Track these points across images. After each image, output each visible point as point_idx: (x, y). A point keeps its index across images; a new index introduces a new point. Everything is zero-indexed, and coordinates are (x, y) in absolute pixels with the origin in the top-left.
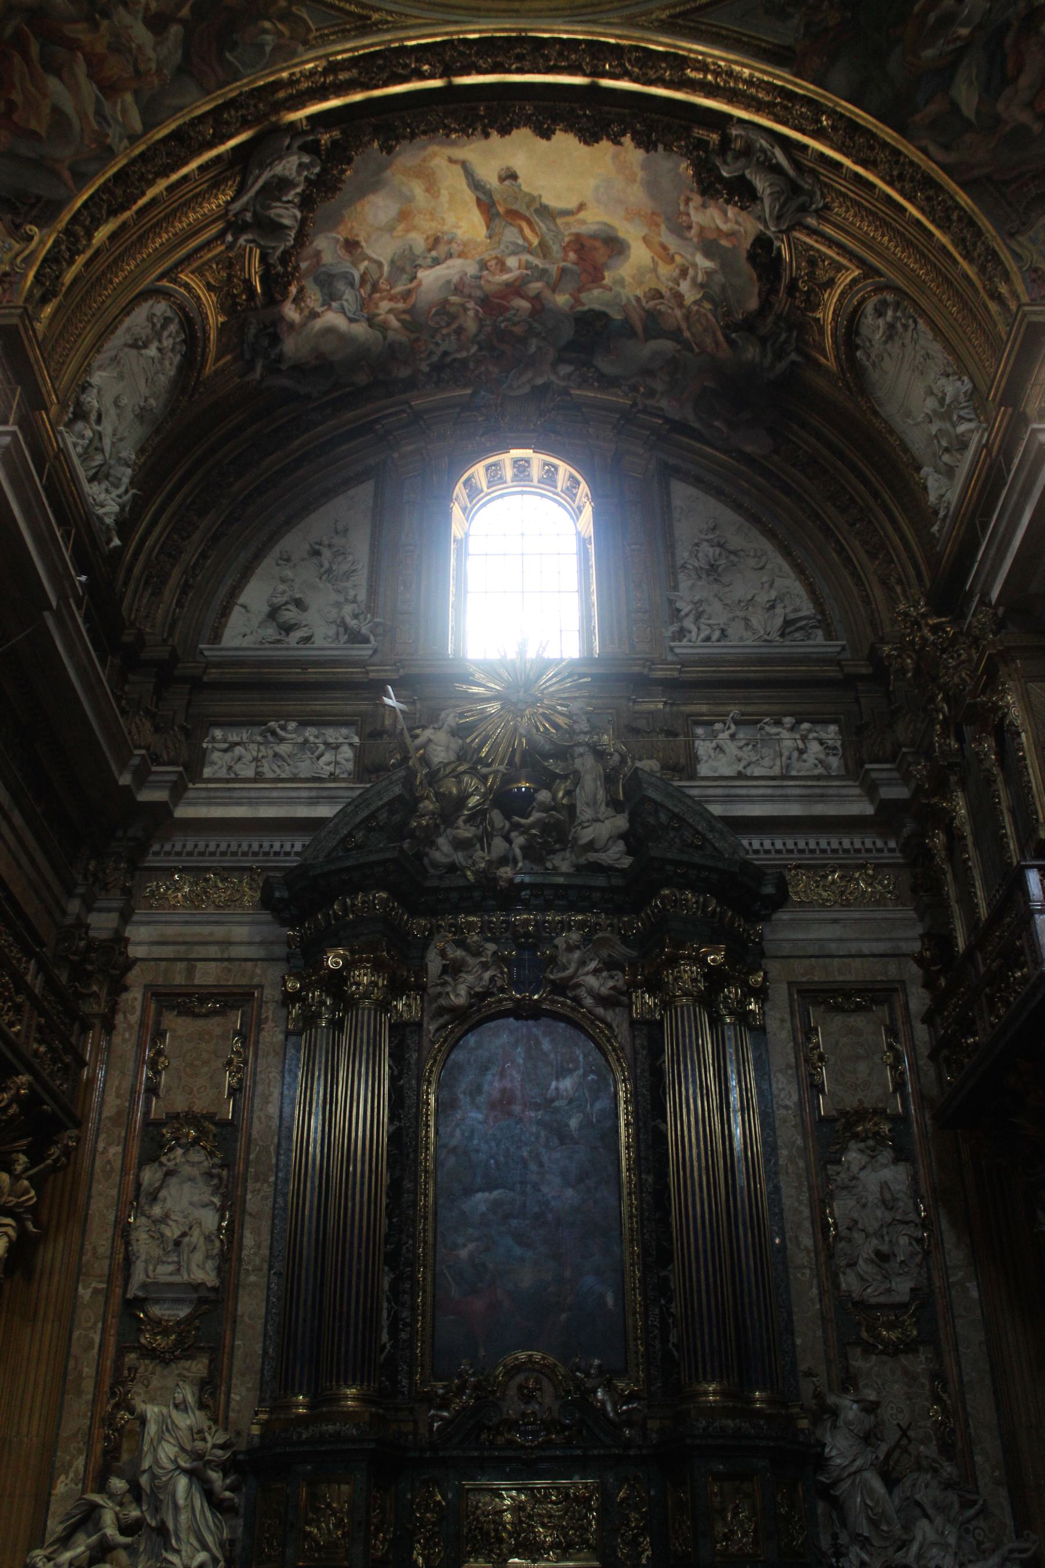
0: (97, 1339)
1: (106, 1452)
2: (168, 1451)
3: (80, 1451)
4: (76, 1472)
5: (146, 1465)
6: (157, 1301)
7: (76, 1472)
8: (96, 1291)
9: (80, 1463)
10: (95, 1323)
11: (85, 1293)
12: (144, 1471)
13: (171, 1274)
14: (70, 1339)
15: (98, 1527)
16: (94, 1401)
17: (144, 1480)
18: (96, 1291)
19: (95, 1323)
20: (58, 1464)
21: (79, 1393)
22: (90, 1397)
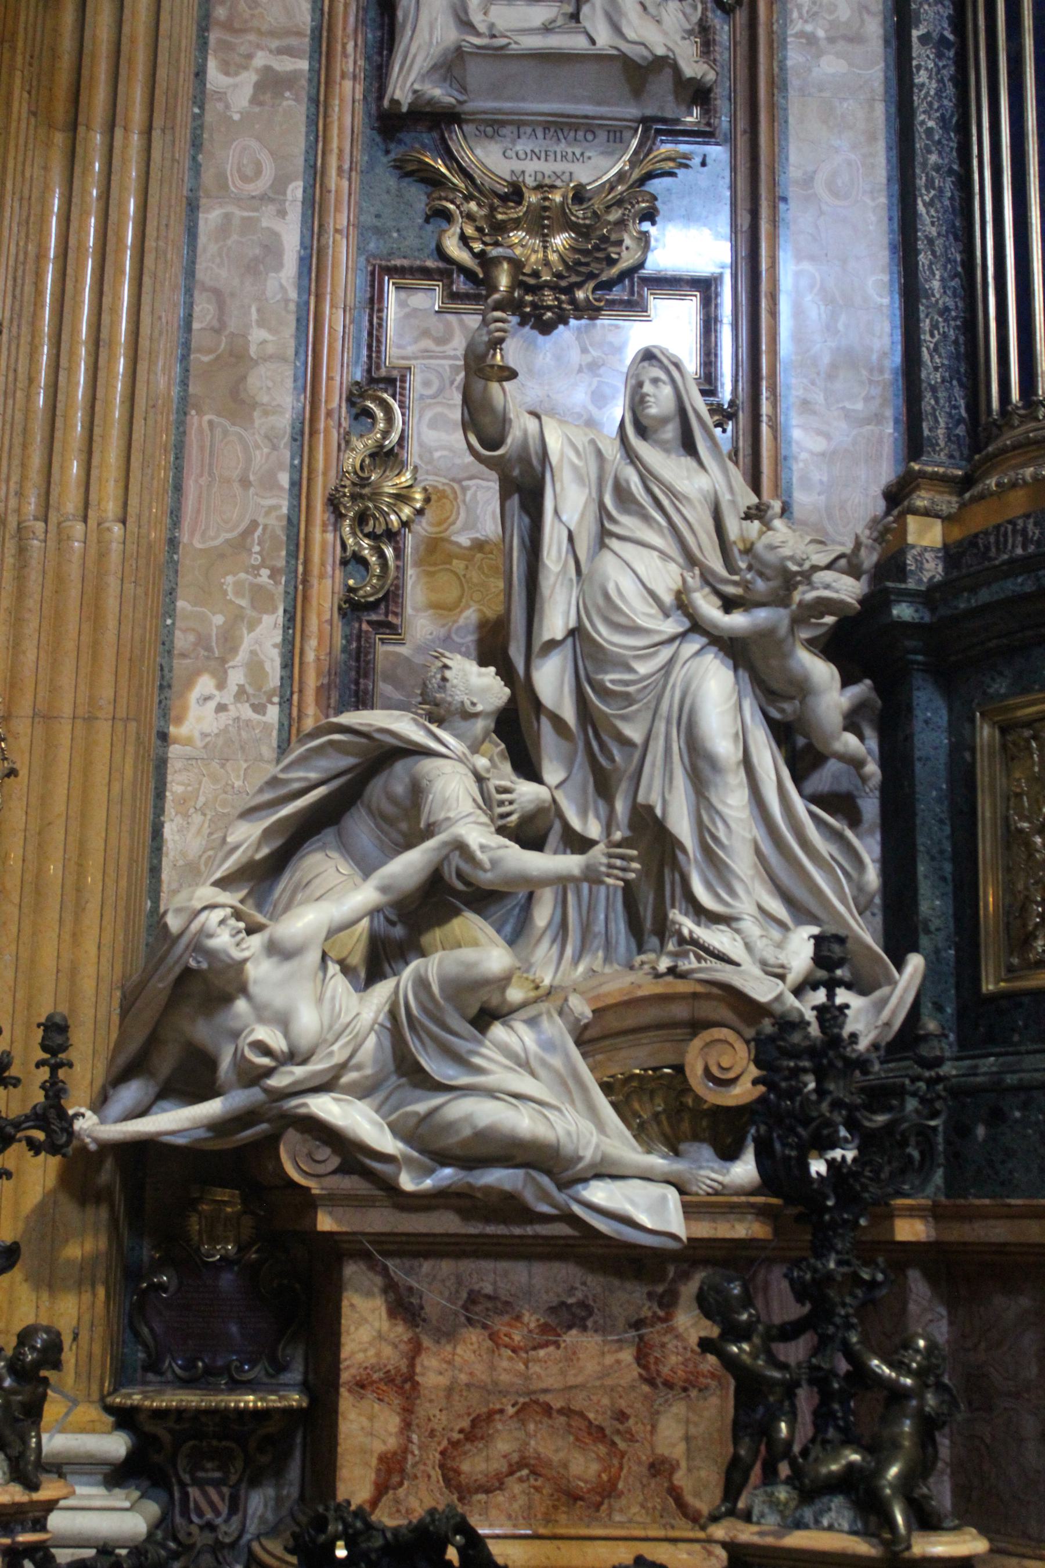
0: (291, 235)
1: (352, 607)
2: (642, 575)
3: (260, 598)
4: (255, 668)
5: (556, 622)
6: (494, 126)
7: (255, 668)
8: (271, 84)
9: (265, 637)
10: (280, 185)
11: (232, 88)
12: (552, 645)
13: (547, 29)
14: (192, 233)
15: (409, 824)
16: (305, 433)
17: (552, 680)
18: (271, 84)
19: (280, 185)
20: (182, 641)
21: (239, 405)
22: (284, 422)
